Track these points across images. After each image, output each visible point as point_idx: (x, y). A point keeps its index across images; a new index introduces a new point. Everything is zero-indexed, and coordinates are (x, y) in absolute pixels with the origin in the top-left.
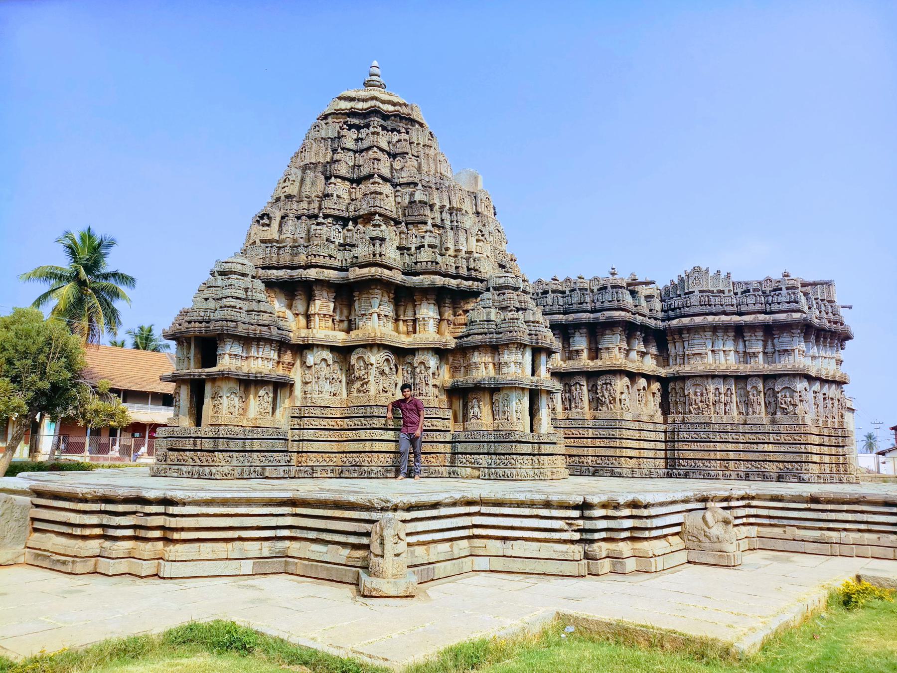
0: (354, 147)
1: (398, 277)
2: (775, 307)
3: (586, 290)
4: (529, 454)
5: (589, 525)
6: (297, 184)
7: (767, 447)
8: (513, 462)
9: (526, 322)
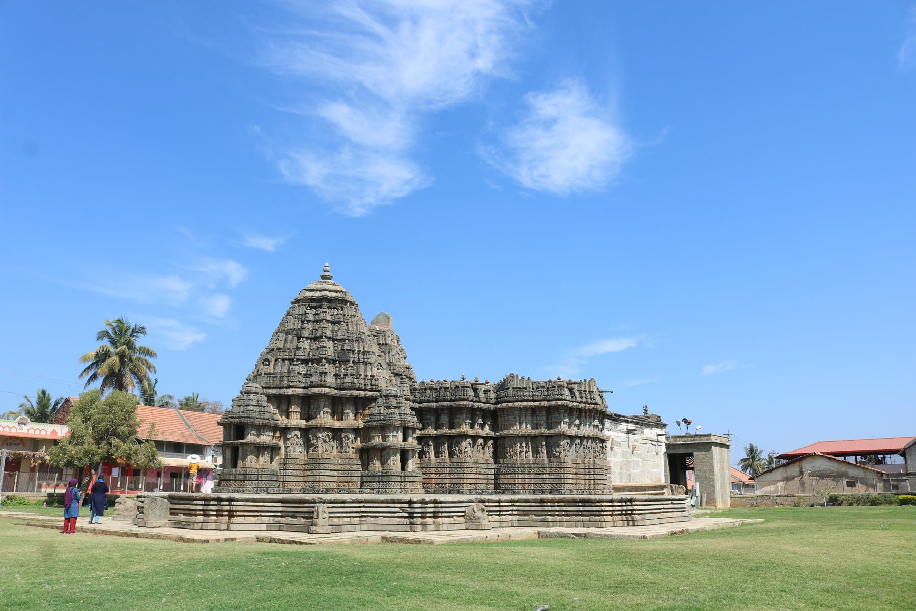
2: (551, 397)
5: (412, 510)
7: (545, 476)
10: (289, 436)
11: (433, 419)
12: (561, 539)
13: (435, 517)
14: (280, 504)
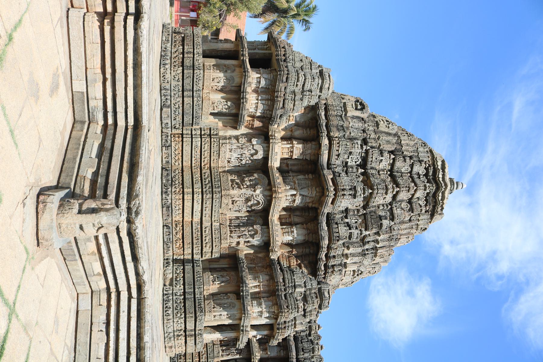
0: (413, 173)
1: (327, 209)
3: (313, 353)
6: (386, 130)
8: (179, 315)
9: (295, 318)
10: (254, 141)
14: (131, 121)
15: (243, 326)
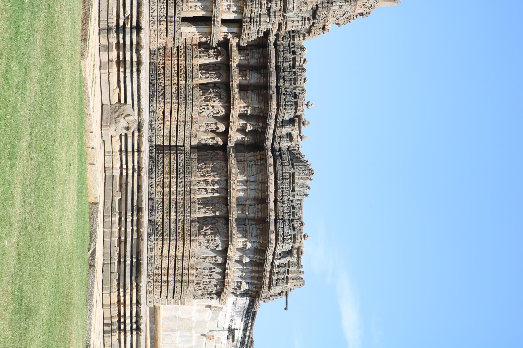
2: (280, 225)
3: (295, 84)
4: (167, 14)
5: (128, 30)
7: (173, 214)
9: (260, 14)
11: (253, 62)
12: (87, 232)
13: (118, 63)
15: (214, 17)
